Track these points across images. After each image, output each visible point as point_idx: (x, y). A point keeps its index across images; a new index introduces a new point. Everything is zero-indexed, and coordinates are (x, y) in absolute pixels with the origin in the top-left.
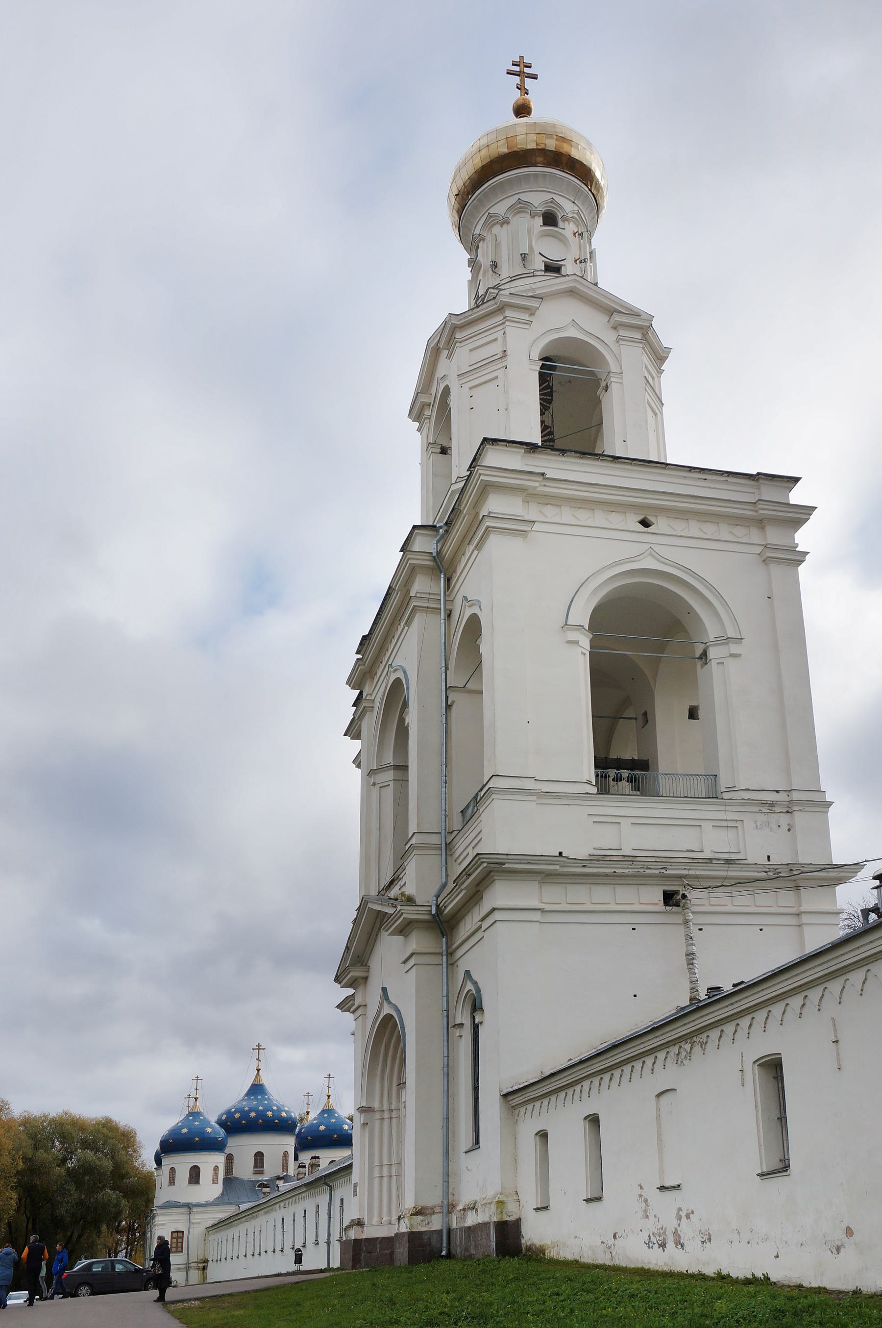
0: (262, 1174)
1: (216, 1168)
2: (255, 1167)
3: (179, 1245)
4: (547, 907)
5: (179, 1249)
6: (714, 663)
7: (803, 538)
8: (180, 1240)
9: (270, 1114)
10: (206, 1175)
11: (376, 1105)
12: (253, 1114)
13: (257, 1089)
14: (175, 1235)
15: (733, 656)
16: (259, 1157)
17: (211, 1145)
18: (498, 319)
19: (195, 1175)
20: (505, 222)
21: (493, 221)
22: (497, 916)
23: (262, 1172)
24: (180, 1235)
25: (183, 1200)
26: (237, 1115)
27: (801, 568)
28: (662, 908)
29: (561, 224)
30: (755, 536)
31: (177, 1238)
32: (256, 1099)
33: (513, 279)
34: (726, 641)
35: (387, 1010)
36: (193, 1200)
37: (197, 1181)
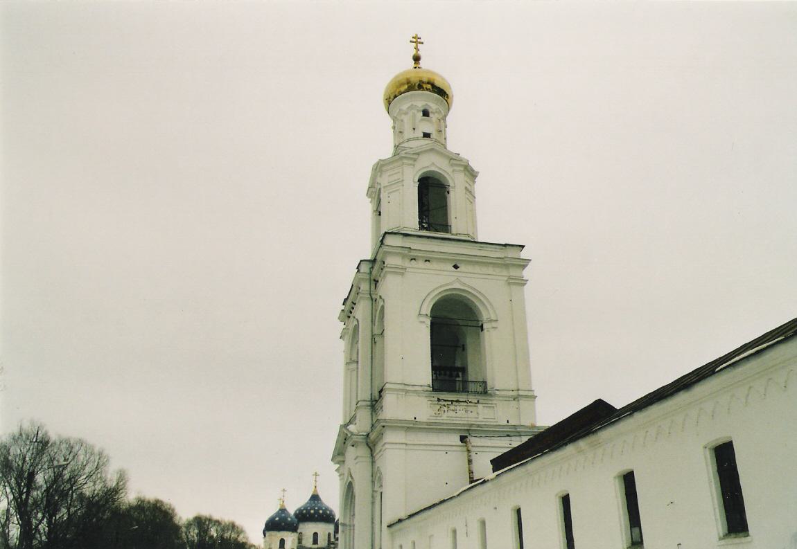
4: (409, 442)
6: (485, 331)
7: (526, 273)
9: (321, 512)
11: (348, 523)
12: (312, 511)
15: (493, 328)
17: (292, 528)
18: (400, 163)
20: (406, 114)
21: (401, 112)
22: (387, 446)
26: (305, 511)
27: (525, 287)
28: (460, 443)
29: (431, 115)
30: (505, 273)
32: (314, 503)
33: (409, 140)
34: (491, 321)
35: (350, 479)
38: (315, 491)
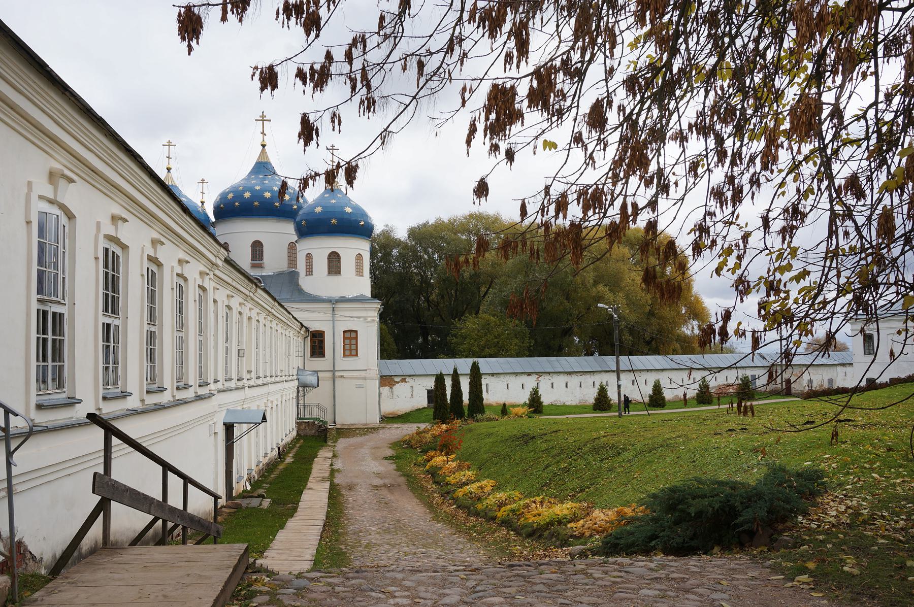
0: (260, 269)
1: (359, 257)
2: (252, 259)
3: (353, 347)
5: (354, 352)
8: (353, 342)
10: (347, 263)
13: (263, 167)
14: (348, 335)
16: (257, 248)
19: (334, 262)
23: (260, 266)
24: (353, 335)
25: (324, 294)
31: (351, 339)
36: (336, 295)
37: (338, 272)
38: (263, 152)
